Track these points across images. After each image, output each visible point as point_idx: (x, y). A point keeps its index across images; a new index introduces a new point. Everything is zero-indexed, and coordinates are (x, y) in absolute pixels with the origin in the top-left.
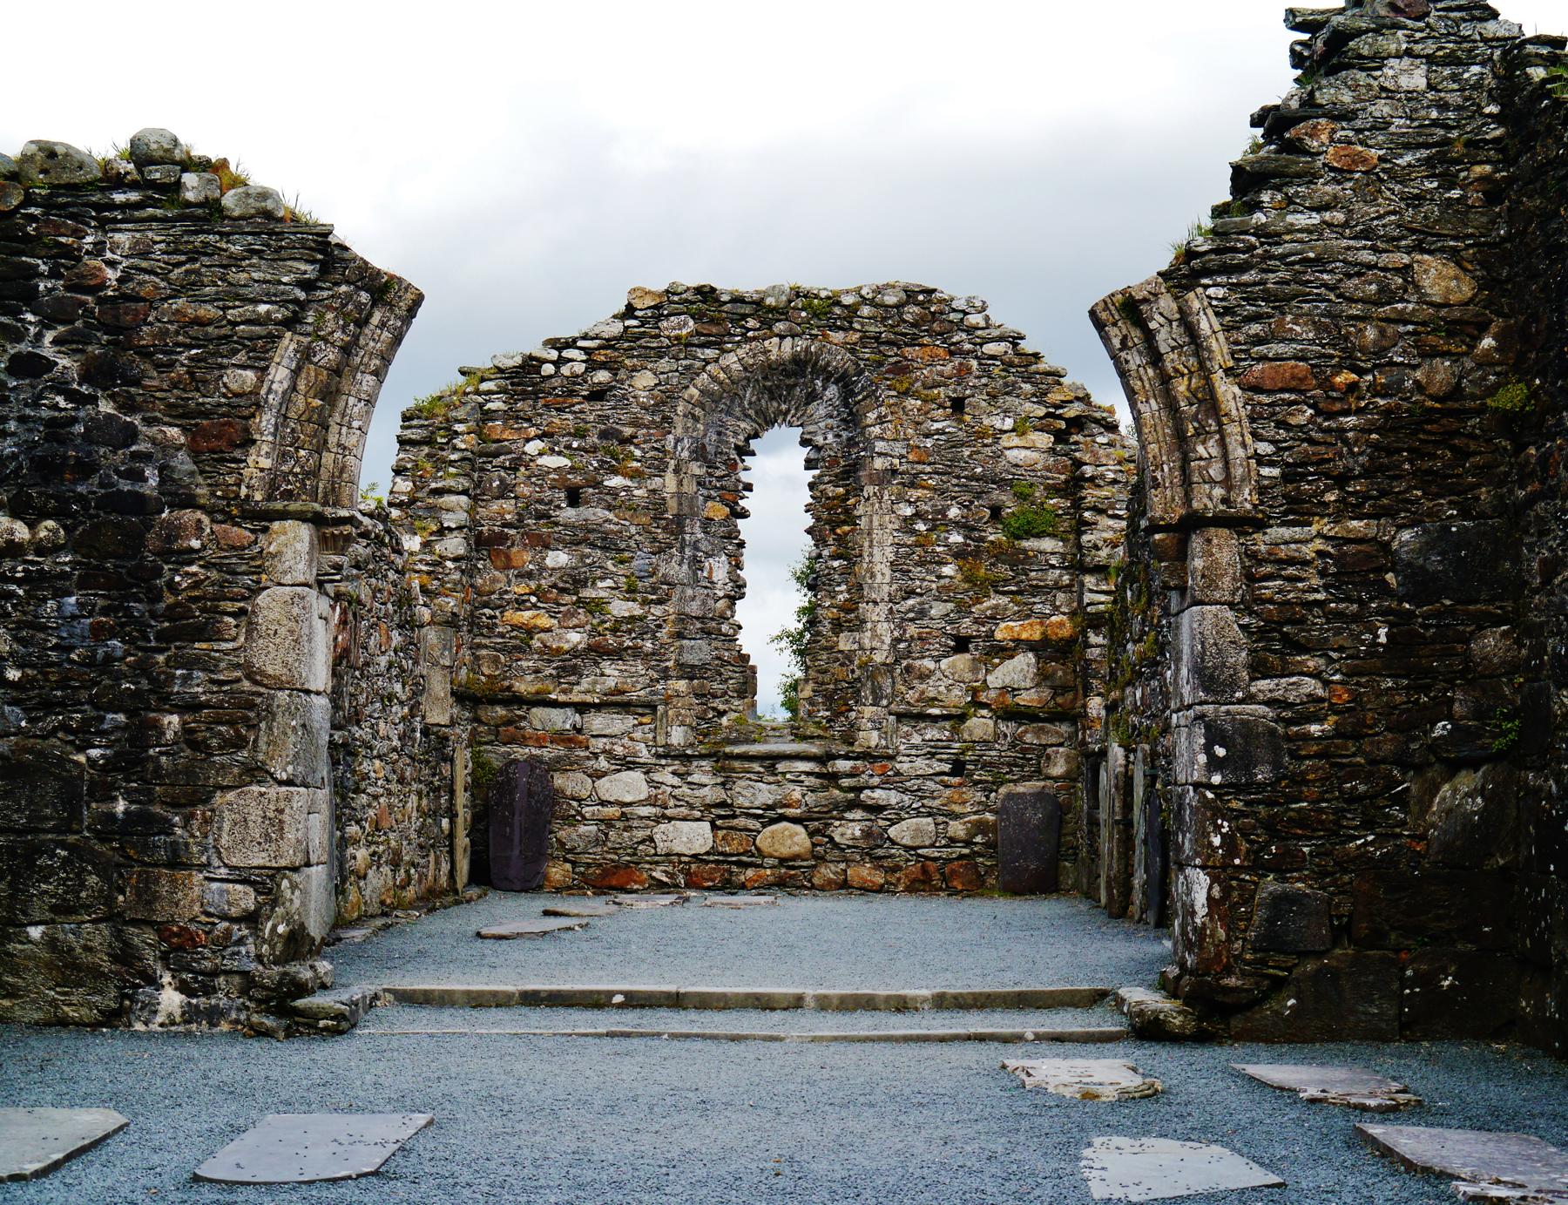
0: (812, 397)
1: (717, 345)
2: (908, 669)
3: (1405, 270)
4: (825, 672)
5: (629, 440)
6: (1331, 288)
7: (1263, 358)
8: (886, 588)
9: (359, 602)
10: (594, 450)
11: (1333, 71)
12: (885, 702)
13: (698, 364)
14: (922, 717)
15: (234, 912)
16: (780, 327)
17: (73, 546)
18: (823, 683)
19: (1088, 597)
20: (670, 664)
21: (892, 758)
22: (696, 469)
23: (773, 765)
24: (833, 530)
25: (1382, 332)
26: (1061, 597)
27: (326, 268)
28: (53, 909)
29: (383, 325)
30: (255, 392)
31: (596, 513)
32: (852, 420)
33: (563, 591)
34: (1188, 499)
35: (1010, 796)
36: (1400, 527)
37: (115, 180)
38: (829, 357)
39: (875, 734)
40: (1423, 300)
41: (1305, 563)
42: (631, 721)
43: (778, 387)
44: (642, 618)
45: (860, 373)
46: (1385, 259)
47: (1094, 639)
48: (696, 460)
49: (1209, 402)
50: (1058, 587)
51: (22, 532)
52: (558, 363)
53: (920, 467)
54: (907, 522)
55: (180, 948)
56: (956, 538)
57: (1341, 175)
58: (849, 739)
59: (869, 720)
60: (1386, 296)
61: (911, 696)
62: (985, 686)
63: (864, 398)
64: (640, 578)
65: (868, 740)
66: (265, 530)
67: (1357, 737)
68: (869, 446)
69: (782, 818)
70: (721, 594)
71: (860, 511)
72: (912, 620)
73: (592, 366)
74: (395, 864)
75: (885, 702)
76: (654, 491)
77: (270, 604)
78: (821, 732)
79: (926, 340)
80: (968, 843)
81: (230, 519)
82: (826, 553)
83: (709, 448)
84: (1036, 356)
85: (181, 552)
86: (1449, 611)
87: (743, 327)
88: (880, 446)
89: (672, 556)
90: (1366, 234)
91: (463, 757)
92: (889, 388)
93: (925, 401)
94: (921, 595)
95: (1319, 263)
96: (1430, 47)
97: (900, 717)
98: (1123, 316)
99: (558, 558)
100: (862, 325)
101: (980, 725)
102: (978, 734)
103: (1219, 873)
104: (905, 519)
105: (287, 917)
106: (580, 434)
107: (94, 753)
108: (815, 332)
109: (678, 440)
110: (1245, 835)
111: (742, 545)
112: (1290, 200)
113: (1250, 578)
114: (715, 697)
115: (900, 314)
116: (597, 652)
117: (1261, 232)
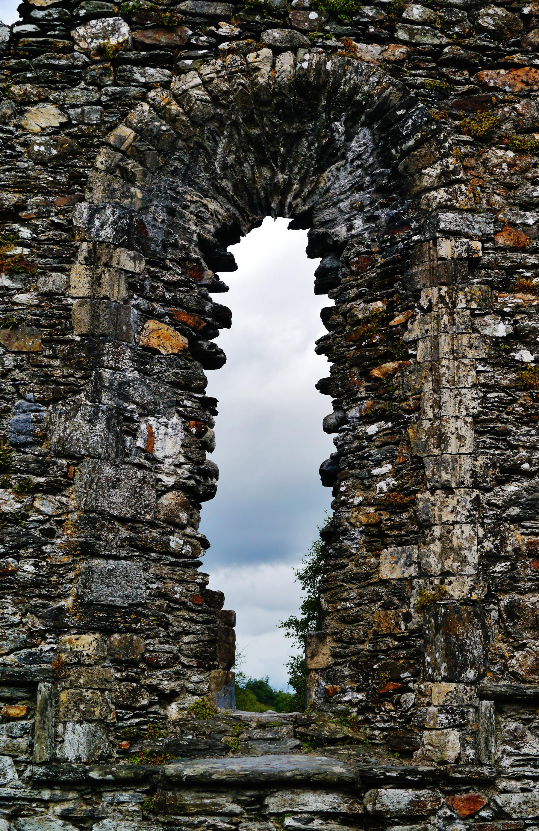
2: (513, 611)
4: (356, 620)
8: (467, 463)
12: (471, 674)
13: (133, 90)
18: (351, 641)
20: (67, 603)
22: (125, 260)
23: (260, 800)
24: (366, 374)
32: (396, 185)
38: (356, 79)
39: (454, 736)
43: (271, 138)
44: (18, 518)
45: (410, 104)
48: (129, 247)
53: (518, 257)
54: (499, 353)
58: (402, 743)
59: (442, 709)
61: (519, 661)
63: (418, 145)
64: (19, 447)
65: (441, 747)
70: (169, 481)
71: (415, 331)
72: (516, 520)
75: (471, 674)
76: (50, 295)
78: (347, 731)
79: (517, 58)
82: (354, 413)
83: (151, 232)
87: (212, 34)
88: (447, 220)
89: (77, 406)
92: (458, 130)
93: (520, 151)
94: (529, 475)
100: (411, 33)
104: (496, 342)
109: (95, 210)
114: (154, 665)
115: (473, 19)
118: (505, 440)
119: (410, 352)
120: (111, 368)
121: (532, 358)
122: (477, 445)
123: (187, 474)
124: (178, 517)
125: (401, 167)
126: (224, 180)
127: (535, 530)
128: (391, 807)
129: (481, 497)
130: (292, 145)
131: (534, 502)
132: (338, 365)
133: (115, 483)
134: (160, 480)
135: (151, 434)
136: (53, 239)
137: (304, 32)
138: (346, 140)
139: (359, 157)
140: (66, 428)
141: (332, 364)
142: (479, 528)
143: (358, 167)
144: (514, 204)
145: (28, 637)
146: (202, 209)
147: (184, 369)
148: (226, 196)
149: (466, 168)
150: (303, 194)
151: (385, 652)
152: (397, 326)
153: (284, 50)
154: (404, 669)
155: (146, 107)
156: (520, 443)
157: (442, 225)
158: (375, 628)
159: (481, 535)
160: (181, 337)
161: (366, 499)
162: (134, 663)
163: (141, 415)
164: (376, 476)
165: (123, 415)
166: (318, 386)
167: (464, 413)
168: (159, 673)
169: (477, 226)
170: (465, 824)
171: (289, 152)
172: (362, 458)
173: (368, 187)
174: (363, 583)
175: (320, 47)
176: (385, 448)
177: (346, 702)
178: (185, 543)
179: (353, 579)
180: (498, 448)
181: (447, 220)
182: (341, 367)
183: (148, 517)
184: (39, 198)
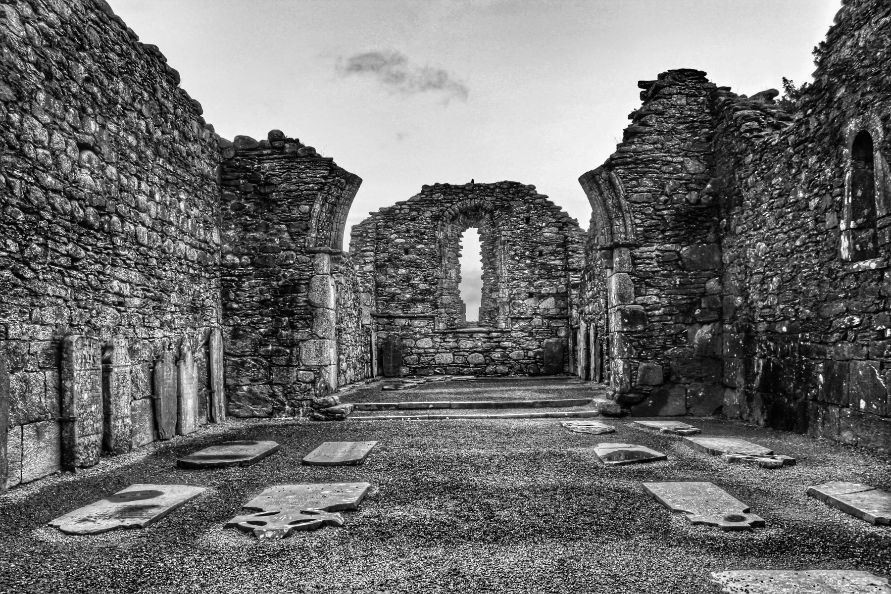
0: (482, 218)
1: (451, 202)
3: (681, 163)
5: (423, 234)
6: (658, 169)
7: (636, 192)
9: (341, 283)
10: (412, 237)
11: (656, 99)
14: (518, 318)
15: (307, 380)
16: (470, 196)
17: (252, 264)
19: (571, 279)
21: (509, 332)
25: (675, 183)
26: (562, 279)
27: (331, 172)
28: (251, 380)
29: (349, 190)
30: (309, 212)
31: (413, 256)
33: (404, 282)
34: (612, 241)
35: (548, 343)
36: (683, 247)
37: (262, 145)
40: (688, 173)
41: (652, 258)
42: (427, 322)
46: (675, 160)
47: (574, 292)
49: (619, 207)
50: (561, 276)
51: (237, 260)
52: (400, 209)
55: (291, 392)
56: (528, 261)
57: (660, 133)
60: (676, 171)
62: (538, 308)
66: (313, 257)
67: (671, 315)
69: (475, 352)
73: (411, 210)
74: (355, 368)
77: (316, 282)
80: (534, 358)
81: (302, 253)
84: (552, 203)
85: (287, 265)
86: (699, 274)
88: (503, 233)
90: (668, 152)
91: (374, 334)
95: (654, 161)
96: (687, 91)
97: (512, 319)
98: (589, 180)
99: (403, 271)
101: (537, 320)
102: (537, 323)
103: (626, 360)
105: (324, 382)
106: (408, 231)
107: (262, 330)
110: (635, 347)
111: (460, 265)
112: (644, 141)
113: (635, 265)
116: (413, 301)
117: (635, 151)
181: (503, 233)
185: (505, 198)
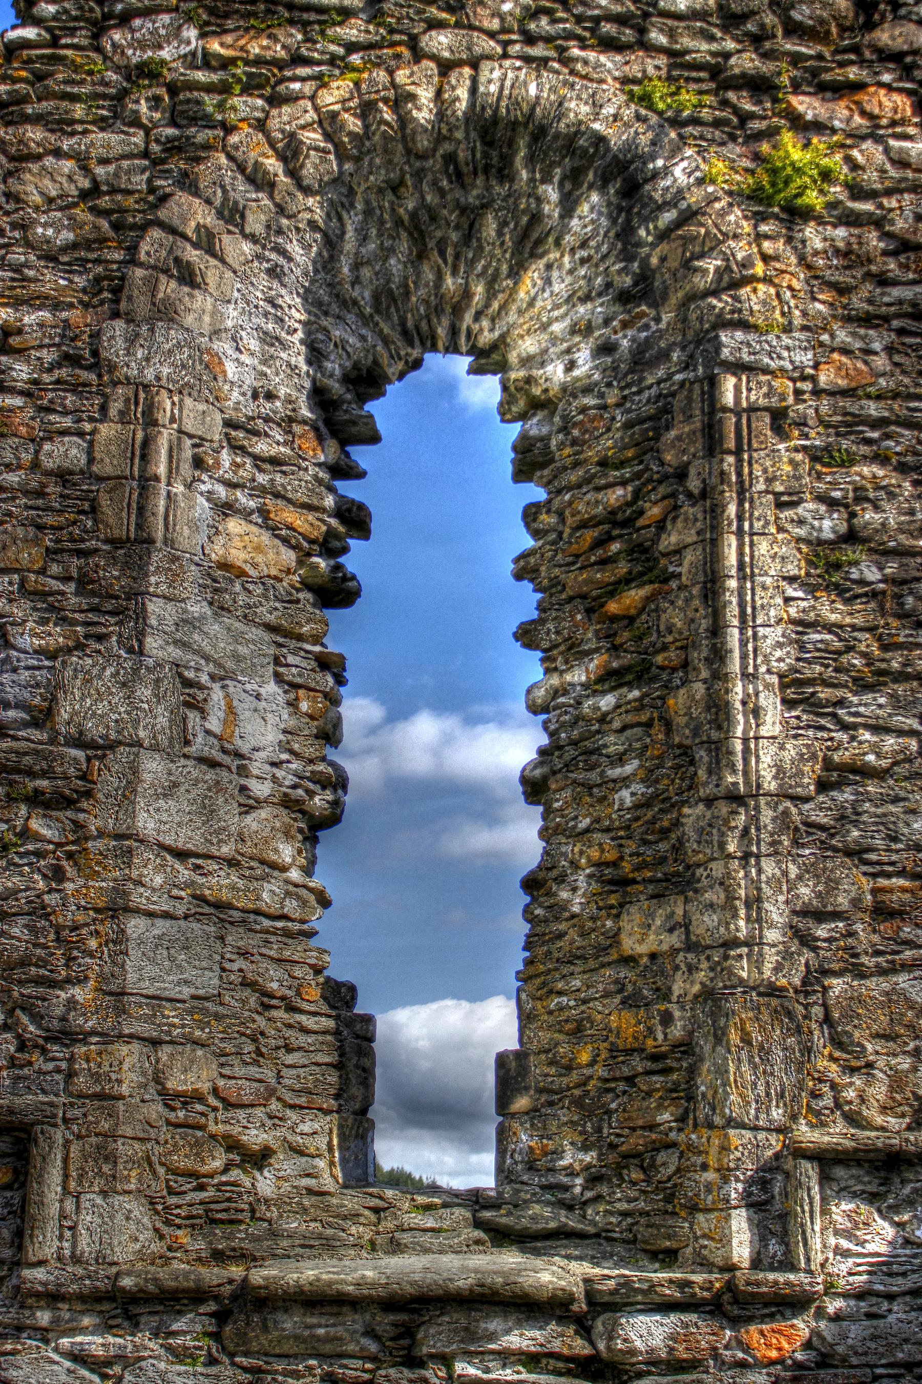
68: (701, 343)
79: (853, 73)
82: (577, 676)
100: (672, 34)
108: (538, 51)
118: (834, 715)
119: (671, 569)
120: (165, 597)
121: (879, 577)
122: (785, 723)
123: (290, 780)
124: (276, 851)
125: (654, 261)
126: (357, 287)
127: (886, 868)
128: (638, 1344)
129: (794, 810)
130: (471, 226)
131: (884, 820)
132: (551, 595)
133: (170, 790)
134: (243, 789)
135: (231, 710)
136: (66, 383)
137: (492, 35)
138: (562, 217)
139: (584, 245)
140: (82, 699)
141: (539, 596)
142: (791, 866)
143: (583, 261)
144: (848, 319)
145: (17, 1051)
146: (320, 336)
147: (289, 602)
148: (361, 315)
149: (766, 258)
150: (491, 310)
151: (630, 1080)
152: (649, 526)
153: (460, 63)
154: (660, 1107)
155: (223, 160)
156: (859, 720)
157: (725, 353)
158: (612, 1039)
159: (792, 876)
160: (283, 549)
161: (597, 820)
162: (198, 1097)
163: (213, 677)
164: (614, 781)
165: (180, 675)
166: (517, 637)
167: (763, 669)
168: (241, 1114)
169: (785, 354)
170: (768, 1374)
171: (467, 238)
172: (589, 752)
173: (600, 295)
174: (592, 964)
175: (518, 58)
176: (628, 733)
177: (565, 1168)
178: (288, 893)
179: (578, 958)
180: (822, 728)
182: (554, 600)
183: (225, 850)
184: (44, 314)
185: (746, 62)
